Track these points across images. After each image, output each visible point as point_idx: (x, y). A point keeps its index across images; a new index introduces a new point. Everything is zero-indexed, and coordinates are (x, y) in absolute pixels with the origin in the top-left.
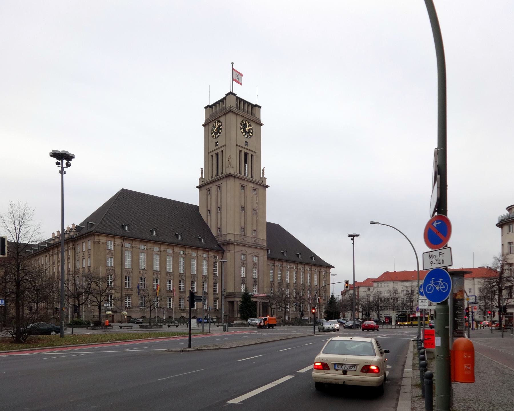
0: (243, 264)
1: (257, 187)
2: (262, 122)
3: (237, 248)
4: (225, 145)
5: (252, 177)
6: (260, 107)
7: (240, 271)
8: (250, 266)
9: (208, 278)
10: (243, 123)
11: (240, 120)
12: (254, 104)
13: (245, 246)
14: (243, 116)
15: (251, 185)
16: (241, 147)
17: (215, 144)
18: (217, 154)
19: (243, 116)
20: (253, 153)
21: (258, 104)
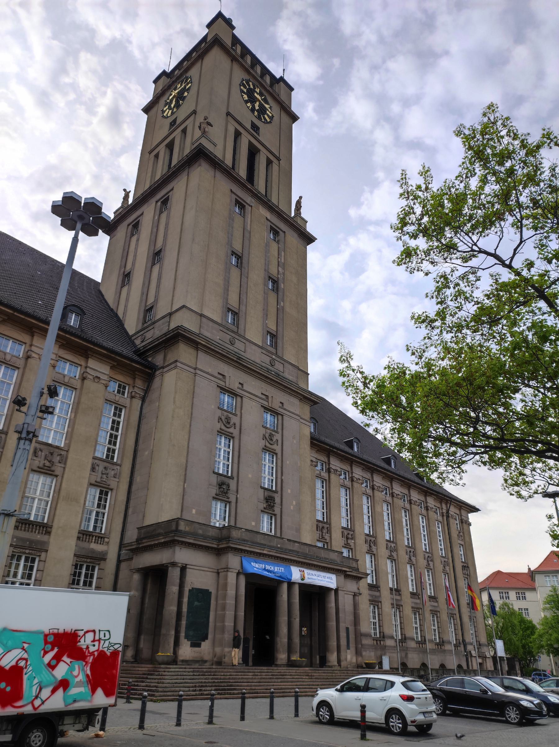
0: (227, 427)
1: (282, 225)
3: (206, 362)
4: (194, 112)
7: (212, 452)
8: (252, 440)
9: (64, 460)
13: (239, 363)
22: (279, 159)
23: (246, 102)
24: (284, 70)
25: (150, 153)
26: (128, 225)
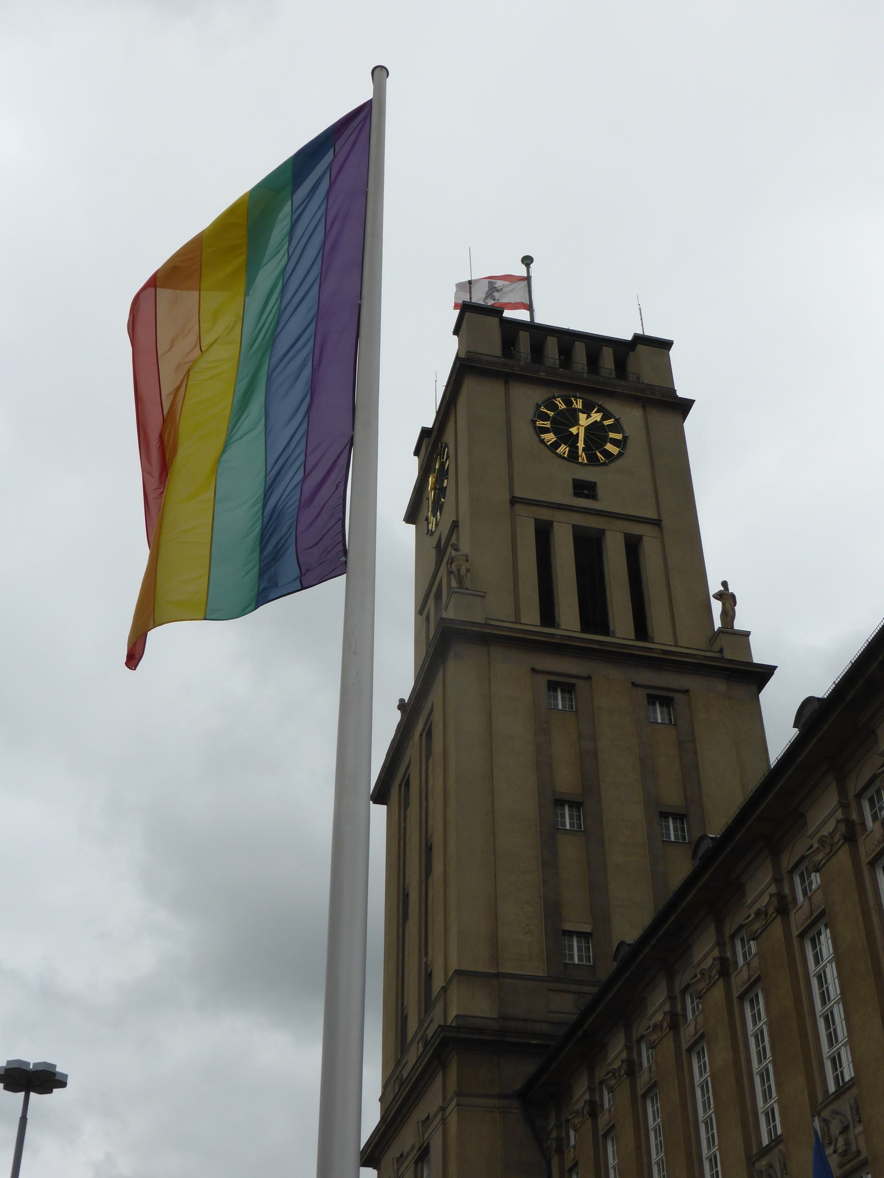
2: (682, 392)
4: (455, 525)
10: (553, 407)
12: (629, 337)
21: (650, 332)
22: (657, 523)
23: (556, 445)
26: (400, 786)
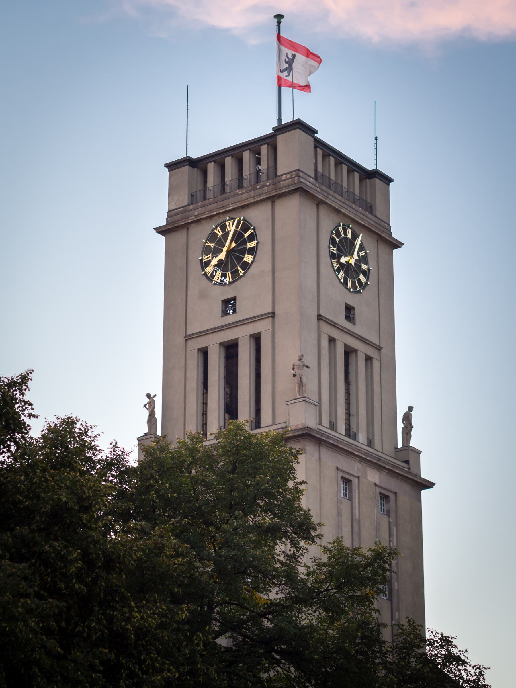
2: (396, 234)
4: (273, 315)
5: (370, 443)
6: (388, 180)
10: (338, 234)
11: (328, 223)
12: (370, 166)
14: (338, 211)
15: (373, 476)
16: (334, 325)
17: (218, 308)
18: (231, 350)
19: (338, 211)
20: (372, 352)
22: (379, 349)
24: (376, 139)
25: (188, 338)
